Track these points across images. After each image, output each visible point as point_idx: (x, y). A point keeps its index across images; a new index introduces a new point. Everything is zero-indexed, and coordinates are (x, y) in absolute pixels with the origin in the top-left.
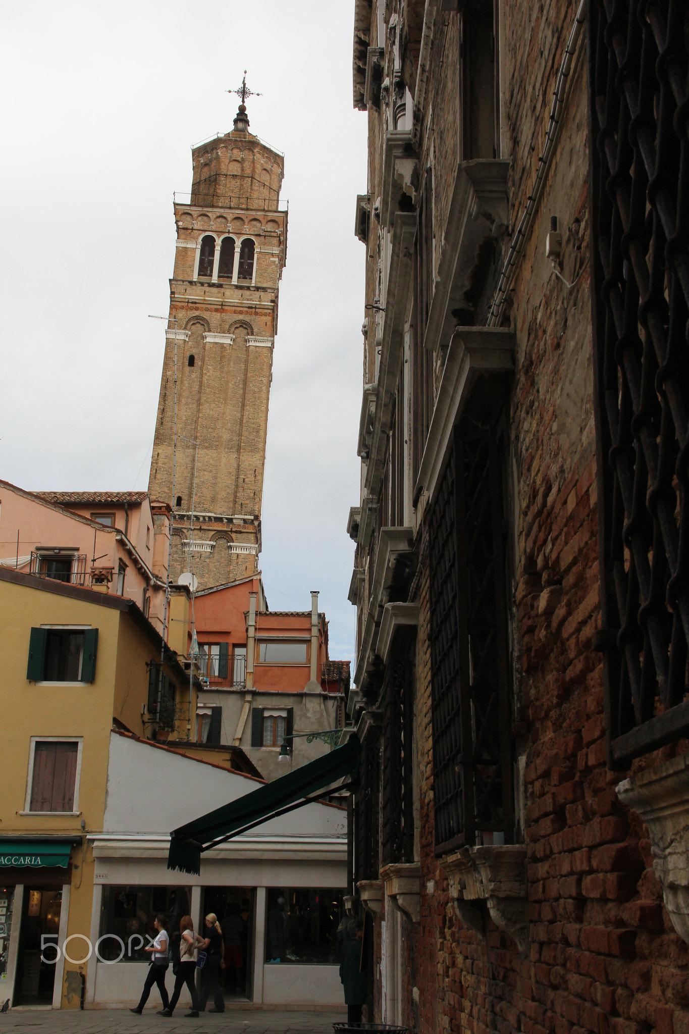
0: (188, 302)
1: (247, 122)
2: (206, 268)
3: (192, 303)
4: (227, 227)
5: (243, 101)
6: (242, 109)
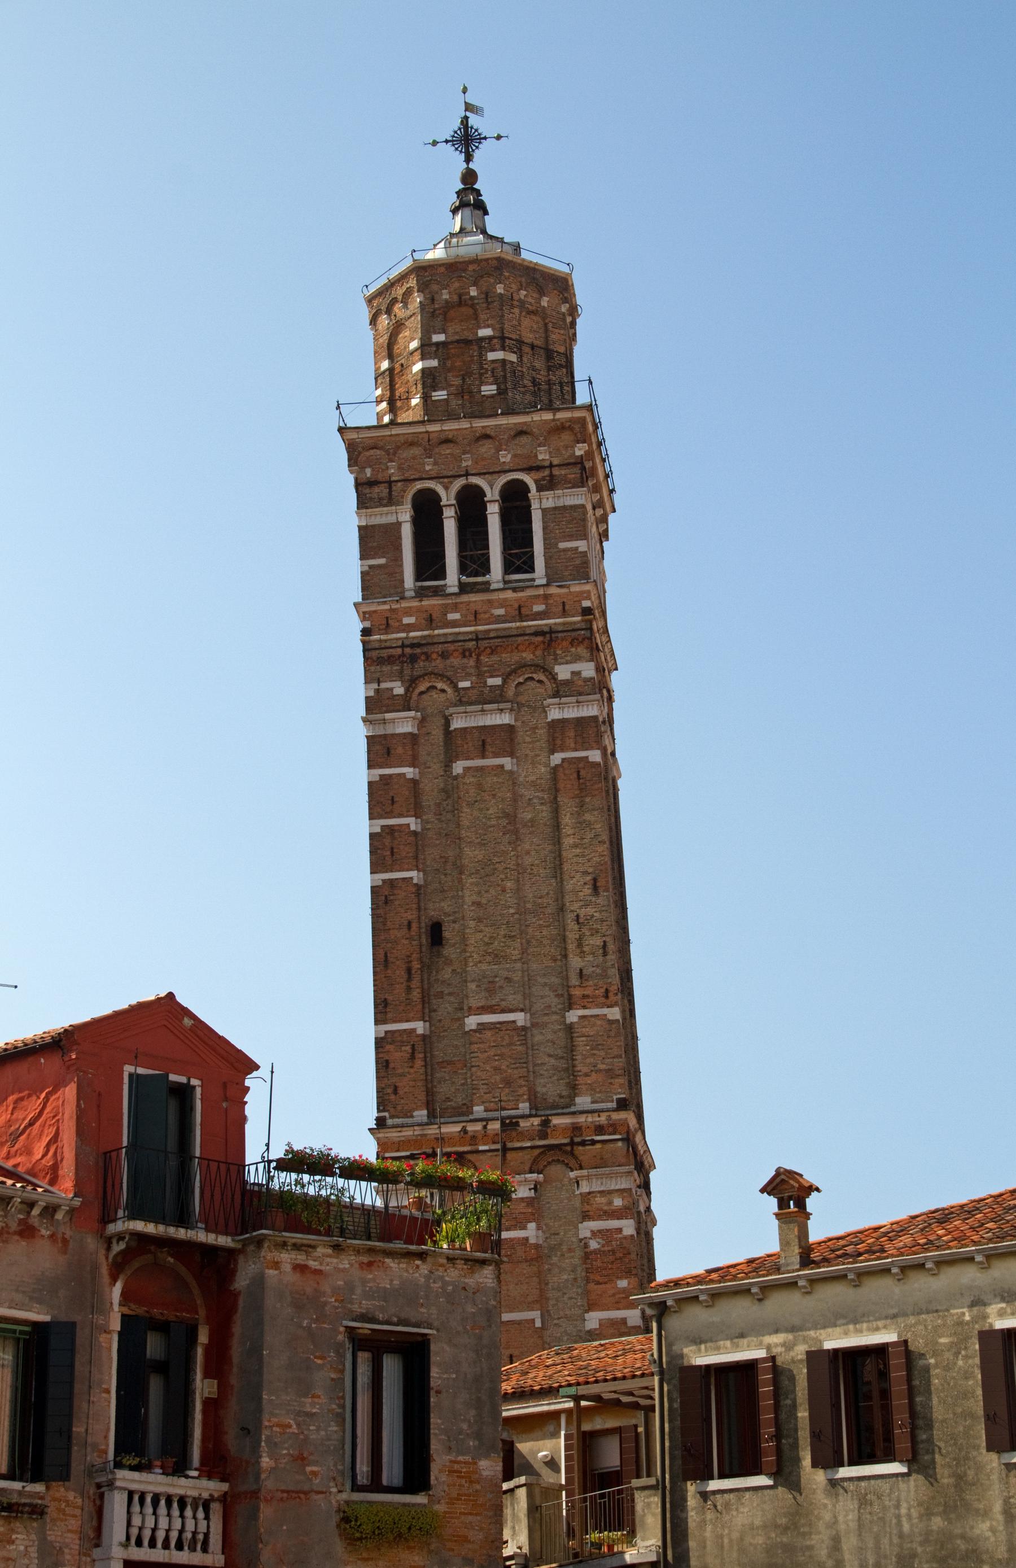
0: (403, 646)
1: (481, 207)
3: (413, 646)
5: (468, 159)
6: (469, 177)
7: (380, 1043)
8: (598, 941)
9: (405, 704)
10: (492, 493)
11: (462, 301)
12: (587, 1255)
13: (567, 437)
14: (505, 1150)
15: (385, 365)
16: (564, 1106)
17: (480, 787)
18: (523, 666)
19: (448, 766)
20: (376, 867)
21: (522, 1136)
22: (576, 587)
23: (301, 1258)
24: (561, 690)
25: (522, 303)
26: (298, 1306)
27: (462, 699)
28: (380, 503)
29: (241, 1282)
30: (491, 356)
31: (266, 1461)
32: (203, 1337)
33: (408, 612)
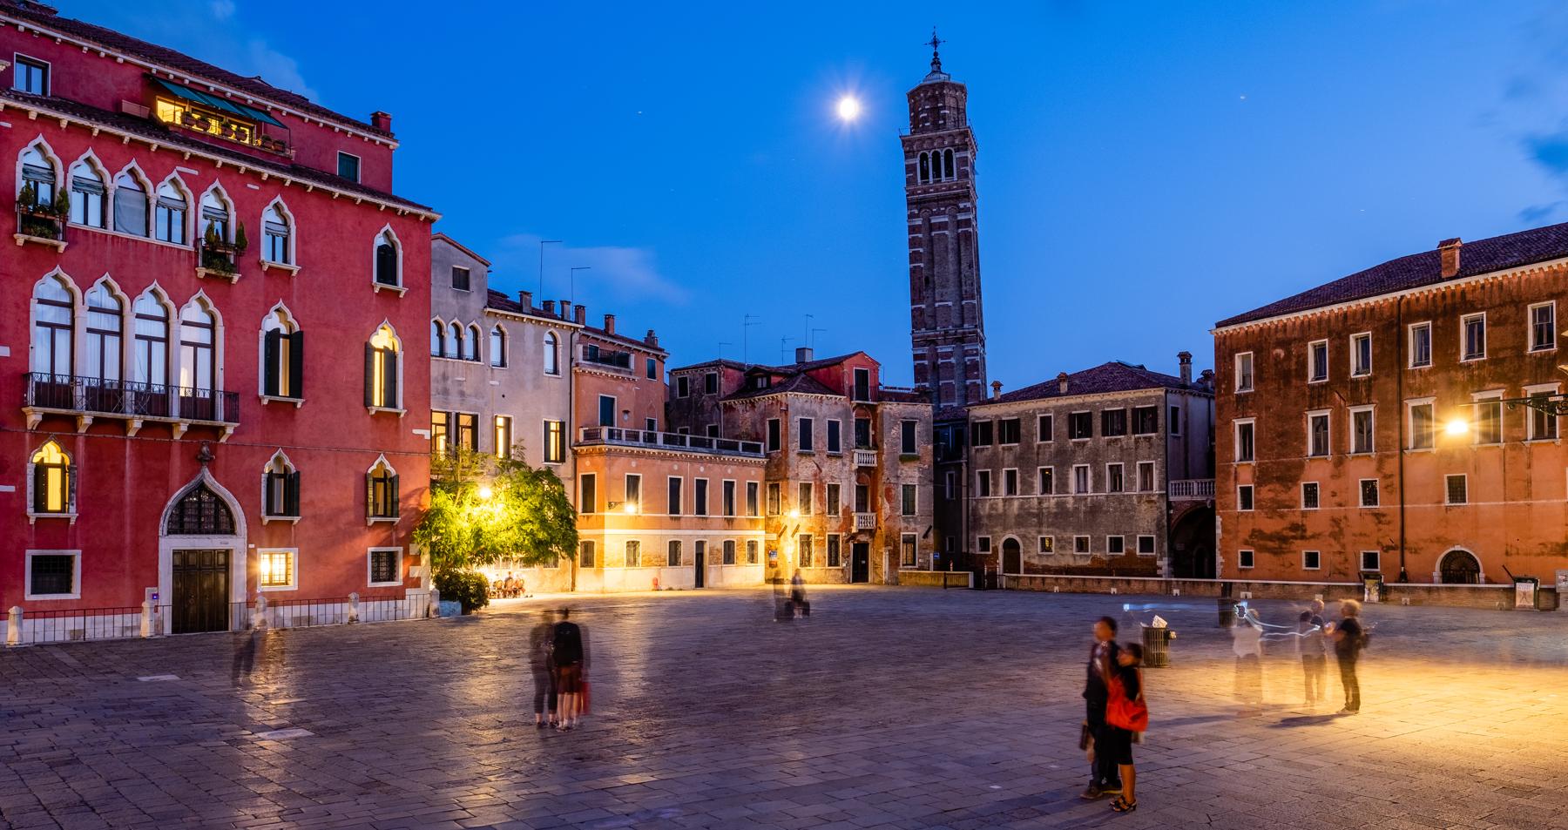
1: (939, 63)
2: (925, 175)
4: (932, 143)
6: (936, 54)
7: (912, 311)
8: (970, 282)
9: (917, 216)
11: (934, 96)
13: (963, 136)
14: (945, 339)
15: (912, 114)
16: (961, 326)
17: (939, 239)
19: (930, 234)
20: (911, 262)
21: (950, 335)
22: (965, 181)
24: (960, 211)
26: (891, 416)
27: (934, 214)
30: (942, 112)
31: (885, 447)
32: (871, 422)
33: (919, 189)
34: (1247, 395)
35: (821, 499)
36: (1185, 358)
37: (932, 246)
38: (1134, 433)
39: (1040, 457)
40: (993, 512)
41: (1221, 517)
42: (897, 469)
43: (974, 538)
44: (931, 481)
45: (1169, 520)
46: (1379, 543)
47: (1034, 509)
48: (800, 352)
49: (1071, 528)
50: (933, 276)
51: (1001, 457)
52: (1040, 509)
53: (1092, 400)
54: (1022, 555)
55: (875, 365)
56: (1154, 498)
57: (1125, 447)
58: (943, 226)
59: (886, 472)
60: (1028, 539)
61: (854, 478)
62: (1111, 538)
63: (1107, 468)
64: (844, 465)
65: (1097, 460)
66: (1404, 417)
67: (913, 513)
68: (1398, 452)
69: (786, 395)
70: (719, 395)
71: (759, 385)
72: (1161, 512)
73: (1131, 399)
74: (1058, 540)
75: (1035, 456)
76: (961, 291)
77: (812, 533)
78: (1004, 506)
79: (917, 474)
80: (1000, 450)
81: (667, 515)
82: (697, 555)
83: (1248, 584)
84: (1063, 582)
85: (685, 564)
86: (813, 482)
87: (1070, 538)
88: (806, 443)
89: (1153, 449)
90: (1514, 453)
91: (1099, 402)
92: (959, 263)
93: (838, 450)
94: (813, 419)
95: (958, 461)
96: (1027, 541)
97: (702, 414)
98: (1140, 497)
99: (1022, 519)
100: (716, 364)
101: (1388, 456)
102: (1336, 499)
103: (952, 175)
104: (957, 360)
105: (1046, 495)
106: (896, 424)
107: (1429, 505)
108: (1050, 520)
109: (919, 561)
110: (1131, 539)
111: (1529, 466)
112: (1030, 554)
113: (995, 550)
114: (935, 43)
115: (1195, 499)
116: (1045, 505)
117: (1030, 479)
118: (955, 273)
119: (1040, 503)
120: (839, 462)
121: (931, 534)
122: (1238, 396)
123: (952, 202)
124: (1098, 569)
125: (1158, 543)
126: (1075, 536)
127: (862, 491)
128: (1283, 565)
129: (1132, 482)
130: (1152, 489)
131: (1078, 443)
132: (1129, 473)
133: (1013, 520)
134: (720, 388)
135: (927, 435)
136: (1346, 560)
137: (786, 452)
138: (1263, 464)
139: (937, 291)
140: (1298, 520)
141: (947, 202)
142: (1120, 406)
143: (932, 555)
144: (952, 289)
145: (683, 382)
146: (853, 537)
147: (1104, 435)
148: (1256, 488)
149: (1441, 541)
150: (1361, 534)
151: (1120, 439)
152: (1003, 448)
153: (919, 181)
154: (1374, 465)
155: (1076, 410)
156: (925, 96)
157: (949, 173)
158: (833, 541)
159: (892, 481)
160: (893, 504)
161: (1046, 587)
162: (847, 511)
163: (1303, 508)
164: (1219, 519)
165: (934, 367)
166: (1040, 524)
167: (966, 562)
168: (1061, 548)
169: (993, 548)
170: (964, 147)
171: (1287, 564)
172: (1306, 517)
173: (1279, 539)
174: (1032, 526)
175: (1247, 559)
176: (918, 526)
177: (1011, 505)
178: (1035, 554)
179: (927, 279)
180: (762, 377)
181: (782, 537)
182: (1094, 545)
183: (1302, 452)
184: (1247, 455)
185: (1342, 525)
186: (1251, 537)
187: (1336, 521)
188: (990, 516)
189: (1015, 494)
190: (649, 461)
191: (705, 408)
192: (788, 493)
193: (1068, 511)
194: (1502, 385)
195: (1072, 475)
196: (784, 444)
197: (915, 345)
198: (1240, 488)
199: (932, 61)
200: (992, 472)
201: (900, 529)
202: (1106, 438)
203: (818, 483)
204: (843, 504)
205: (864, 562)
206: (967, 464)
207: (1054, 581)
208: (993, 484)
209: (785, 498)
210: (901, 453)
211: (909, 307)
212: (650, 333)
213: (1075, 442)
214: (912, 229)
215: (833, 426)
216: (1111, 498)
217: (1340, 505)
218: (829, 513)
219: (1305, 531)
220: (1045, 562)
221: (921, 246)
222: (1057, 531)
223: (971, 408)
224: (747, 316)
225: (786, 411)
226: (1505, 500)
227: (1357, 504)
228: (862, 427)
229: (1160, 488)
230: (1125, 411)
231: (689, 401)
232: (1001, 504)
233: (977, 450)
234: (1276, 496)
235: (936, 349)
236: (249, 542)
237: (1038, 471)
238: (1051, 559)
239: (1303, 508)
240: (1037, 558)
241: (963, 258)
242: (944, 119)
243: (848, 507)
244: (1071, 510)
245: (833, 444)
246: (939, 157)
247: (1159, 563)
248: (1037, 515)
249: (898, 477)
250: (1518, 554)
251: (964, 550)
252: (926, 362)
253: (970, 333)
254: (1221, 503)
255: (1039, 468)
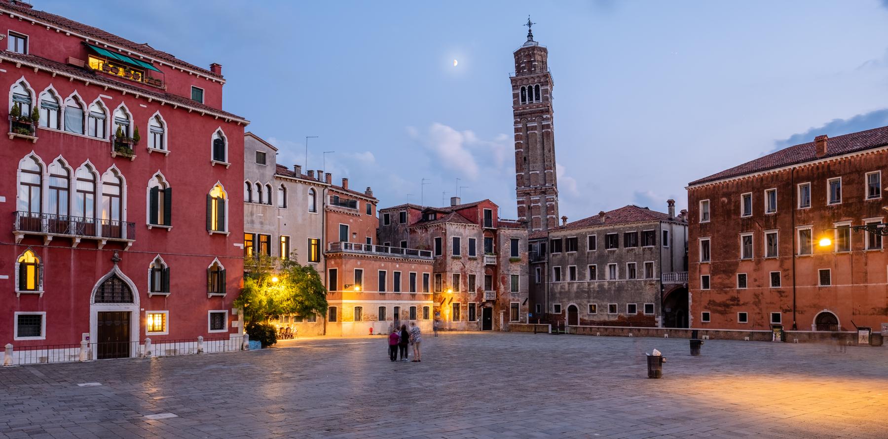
2: (524, 99)
4: (528, 82)
6: (530, 31)
7: (517, 176)
9: (520, 122)
10: (534, 87)
12: (547, 207)
13: (545, 77)
15: (517, 65)
17: (532, 136)
18: (538, 116)
23: (504, 230)
24: (544, 119)
25: (538, 54)
26: (504, 236)
27: (528, 121)
28: (516, 89)
29: (498, 233)
30: (533, 63)
31: (501, 253)
32: (493, 239)
34: (706, 224)
35: (465, 283)
36: (671, 203)
37: (528, 139)
38: (642, 246)
39: (589, 259)
40: (563, 290)
41: (692, 293)
42: (508, 266)
43: (551, 305)
44: (527, 273)
45: (662, 295)
46: (781, 308)
47: (586, 288)
48: (453, 199)
49: (606, 299)
50: (529, 156)
51: (566, 259)
52: (589, 289)
53: (618, 227)
54: (579, 314)
55: (495, 207)
56: (654, 283)
57: (637, 253)
58: (534, 128)
59: (501, 267)
60: (582, 306)
61: (483, 271)
62: (629, 305)
63: (627, 265)
64: (478, 263)
65: (621, 261)
66: (795, 236)
67: (517, 291)
68: (792, 256)
69: (445, 224)
70: (407, 224)
71: (430, 219)
72: (657, 290)
73: (641, 226)
74: (599, 306)
75: (586, 258)
76: (544, 165)
77: (460, 302)
78: (569, 287)
79: (519, 269)
80: (566, 255)
81: (378, 292)
82: (395, 314)
83: (707, 331)
84: (602, 330)
85: (388, 320)
86: (460, 273)
87: (606, 305)
88: (456, 250)
89: (653, 255)
90: (857, 257)
91: (622, 228)
92: (543, 149)
93: (475, 255)
94: (461, 237)
95: (542, 261)
96: (582, 307)
97: (398, 235)
98: (646, 282)
99: (579, 294)
100: (406, 207)
101: (786, 259)
102: (757, 283)
103: (539, 99)
104: (542, 204)
105: (592, 281)
106: (507, 240)
107: (809, 286)
108: (595, 295)
109: (520, 318)
110: (641, 306)
111: (866, 264)
112: (583, 314)
113: (564, 312)
114: (530, 24)
115: (676, 283)
116: (592, 286)
117: (583, 272)
118: (540, 155)
119: (589, 285)
120: (475, 262)
121: (527, 303)
122: (701, 224)
123: (539, 114)
124: (622, 322)
125: (656, 308)
126: (609, 304)
127: (488, 278)
128: (727, 320)
129: (641, 273)
130: (652, 277)
131: (611, 251)
132: (639, 268)
133: (574, 295)
134: (407, 220)
135: (525, 247)
136: (762, 318)
137: (445, 256)
138: (716, 263)
139: (531, 165)
140: (735, 295)
141: (537, 114)
142: (634, 230)
143: (527, 314)
144: (539, 164)
145: (387, 217)
146: (483, 304)
147: (625, 247)
148: (711, 276)
149: (816, 307)
150: (771, 303)
151: (634, 249)
152: (568, 254)
153: (521, 102)
154: (778, 264)
155: (609, 232)
156: (524, 54)
157: (538, 98)
158: (472, 307)
159: (505, 273)
160: (506, 286)
161: (592, 333)
162: (479, 290)
163: (738, 288)
164: (690, 294)
165: (529, 208)
166: (589, 297)
167: (547, 319)
168: (601, 311)
169: (562, 312)
170: (546, 83)
171: (729, 320)
172: (740, 293)
173: (724, 306)
174: (584, 298)
175: (706, 317)
176: (520, 298)
177: (572, 286)
178: (586, 314)
179: (525, 159)
180: (432, 214)
181: (443, 305)
182: (620, 309)
183: (737, 256)
184: (706, 257)
185: (760, 298)
186: (708, 304)
187: (756, 296)
188: (560, 293)
189: (575, 280)
190: (367, 261)
191: (399, 231)
192: (446, 279)
193: (605, 290)
194: (851, 218)
195: (607, 269)
196: (444, 252)
197: (518, 195)
198: (702, 276)
199: (528, 35)
200: (562, 268)
201: (510, 300)
202: (626, 248)
203: (463, 274)
204: (477, 286)
205: (489, 319)
206: (548, 263)
207: (597, 330)
208: (562, 275)
209: (444, 282)
210: (511, 257)
211: (515, 174)
212: (368, 189)
213: (609, 251)
214: (517, 130)
215: (472, 242)
216: (629, 283)
217: (759, 286)
218: (470, 291)
219: (739, 301)
220: (592, 319)
221: (521, 140)
222: (599, 301)
223: (550, 231)
224: (423, 179)
225: (445, 234)
226: (852, 283)
227: (769, 286)
228: (488, 242)
229: (657, 277)
230: (637, 233)
231: (390, 227)
232: (567, 286)
233: (553, 255)
234: (723, 281)
235: (530, 198)
236: (141, 307)
237: (588, 267)
238: (595, 317)
239: (738, 288)
240: (587, 316)
241: (545, 146)
242: (535, 68)
243: (480, 287)
244: (606, 289)
245: (472, 252)
246: (532, 89)
247: (656, 319)
248: (588, 292)
249: (508, 270)
250: (860, 314)
251: (546, 312)
252: (524, 205)
253: (549, 189)
254: (691, 285)
255: (588, 265)
